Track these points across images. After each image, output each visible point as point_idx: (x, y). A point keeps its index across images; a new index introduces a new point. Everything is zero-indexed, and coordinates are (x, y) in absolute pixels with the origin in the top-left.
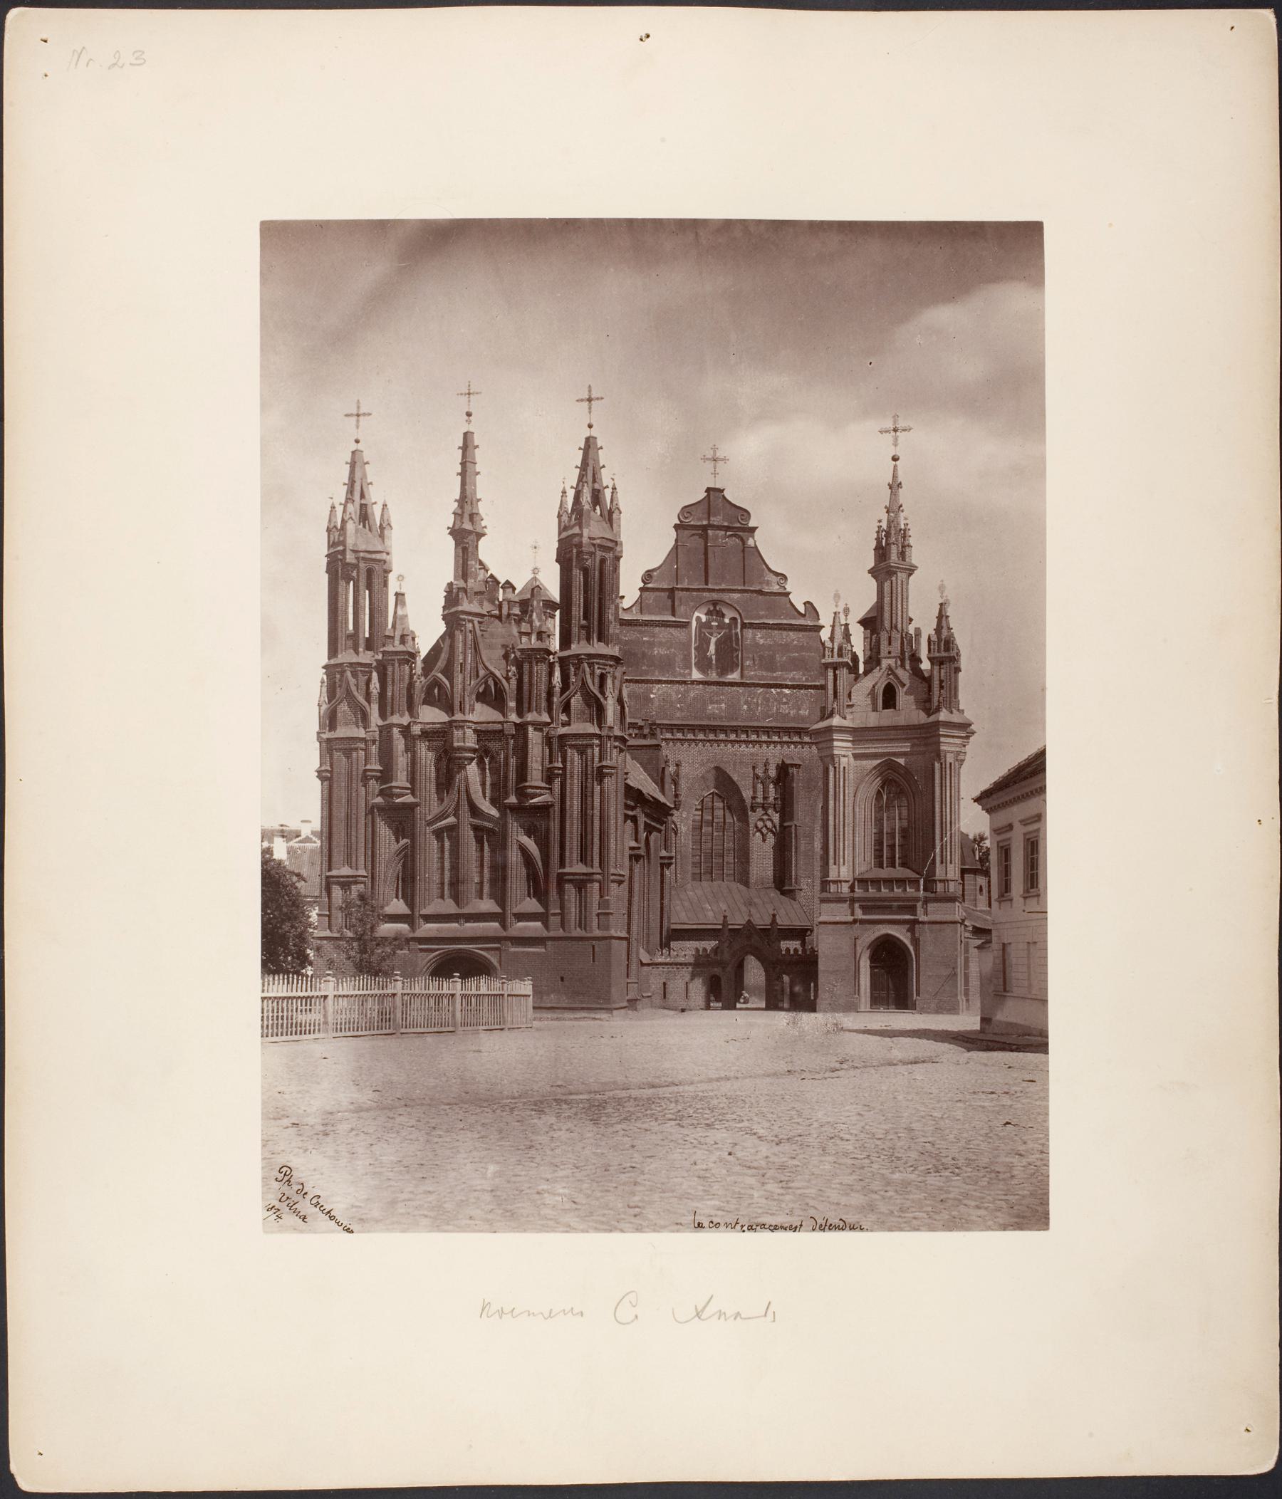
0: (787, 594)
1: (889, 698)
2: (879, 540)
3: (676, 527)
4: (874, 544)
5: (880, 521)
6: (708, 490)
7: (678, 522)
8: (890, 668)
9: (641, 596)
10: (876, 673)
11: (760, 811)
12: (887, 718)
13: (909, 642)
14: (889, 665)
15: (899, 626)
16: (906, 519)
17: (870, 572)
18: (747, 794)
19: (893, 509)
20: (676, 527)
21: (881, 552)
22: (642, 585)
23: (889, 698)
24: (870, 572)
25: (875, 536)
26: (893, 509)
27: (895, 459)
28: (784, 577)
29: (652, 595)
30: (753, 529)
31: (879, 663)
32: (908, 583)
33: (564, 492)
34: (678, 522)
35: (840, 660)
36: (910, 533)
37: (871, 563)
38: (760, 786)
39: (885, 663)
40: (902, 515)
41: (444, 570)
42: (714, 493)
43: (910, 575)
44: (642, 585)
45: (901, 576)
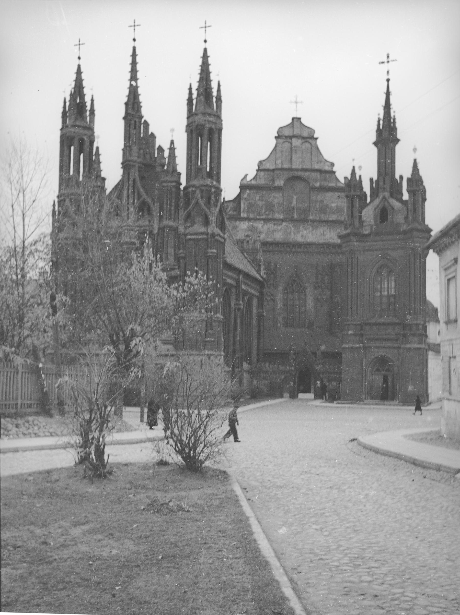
0: (335, 172)
2: (379, 125)
3: (276, 138)
4: (376, 127)
5: (379, 114)
8: (384, 198)
9: (256, 175)
19: (387, 106)
20: (276, 138)
21: (379, 132)
26: (387, 106)
27: (388, 80)
28: (333, 165)
29: (262, 173)
30: (317, 139)
36: (397, 121)
40: (392, 111)
42: (296, 120)
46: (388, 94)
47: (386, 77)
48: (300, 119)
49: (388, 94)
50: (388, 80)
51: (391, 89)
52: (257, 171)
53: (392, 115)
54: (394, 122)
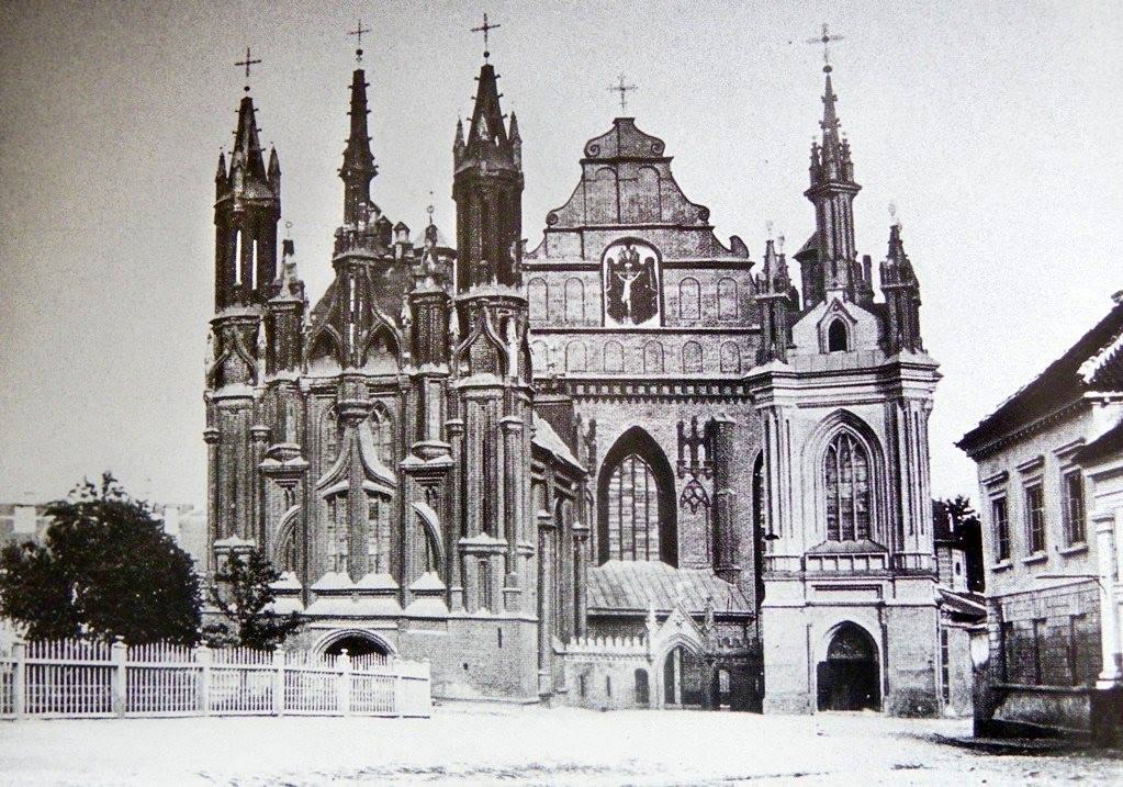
0: (713, 228)
1: (838, 337)
2: (815, 157)
3: (583, 162)
4: (809, 163)
5: (814, 138)
6: (617, 121)
7: (584, 157)
10: (822, 309)
11: (689, 477)
12: (839, 360)
13: (858, 273)
14: (836, 299)
15: (845, 254)
16: (844, 134)
17: (806, 194)
18: (673, 460)
19: (830, 122)
20: (583, 162)
21: (818, 173)
22: (546, 226)
23: (838, 337)
24: (806, 194)
25: (810, 154)
26: (830, 122)
27: (828, 69)
30: (669, 160)
31: (823, 297)
32: (851, 205)
33: (460, 125)
34: (584, 157)
35: (777, 295)
36: (850, 149)
37: (807, 185)
38: (687, 447)
39: (830, 296)
40: (840, 130)
41: (334, 215)
43: (853, 196)
44: (546, 226)
45: (844, 197)
46: (829, 100)
47: (824, 65)
48: (633, 119)
49: (829, 100)
50: (828, 69)
51: (835, 91)
52: (545, 232)
53: (841, 138)
54: (846, 153)
